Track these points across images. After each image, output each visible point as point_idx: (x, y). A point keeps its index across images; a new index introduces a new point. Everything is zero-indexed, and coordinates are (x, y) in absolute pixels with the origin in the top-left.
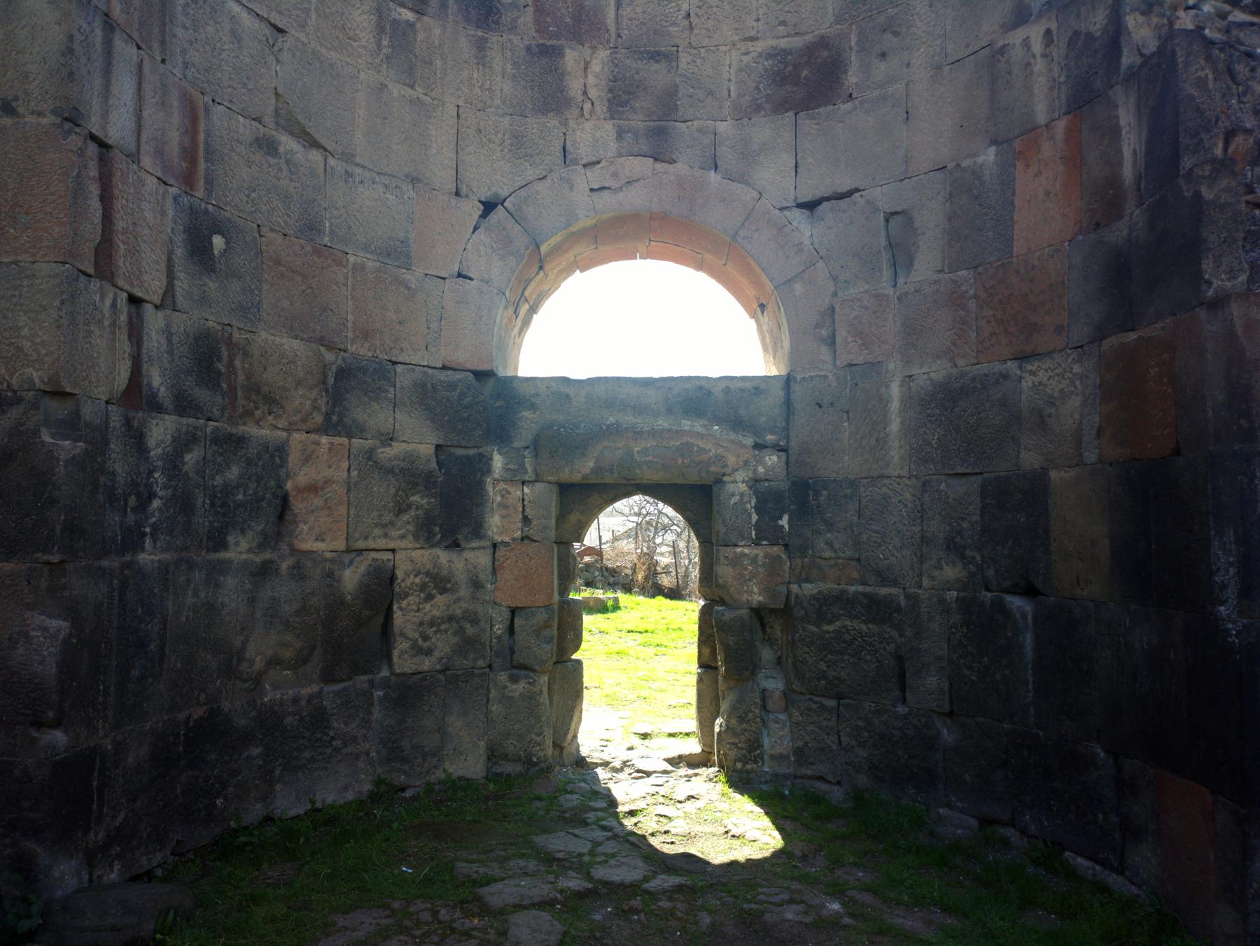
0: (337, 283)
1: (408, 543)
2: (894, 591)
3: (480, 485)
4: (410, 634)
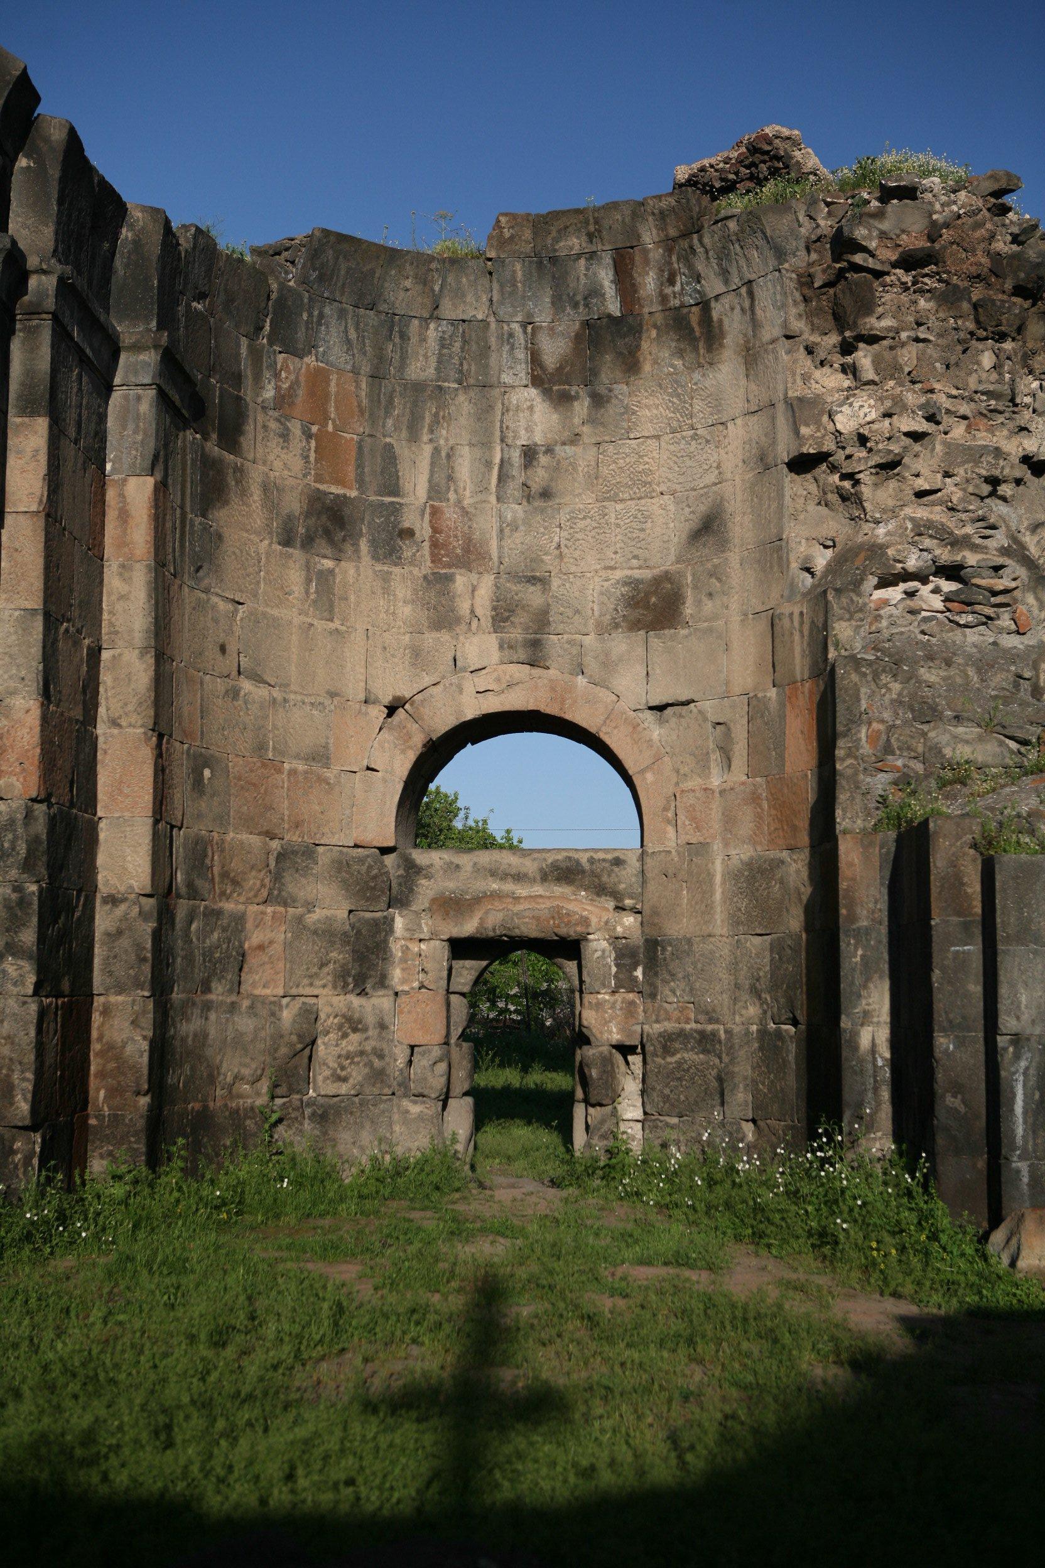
2: (716, 1026)
3: (385, 941)
4: (331, 1064)
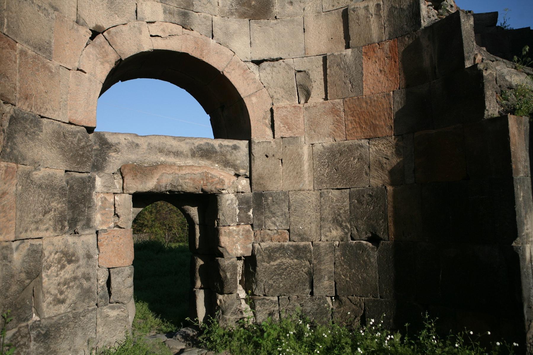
0: (11, 60)
1: (50, 233)
2: (307, 243)
